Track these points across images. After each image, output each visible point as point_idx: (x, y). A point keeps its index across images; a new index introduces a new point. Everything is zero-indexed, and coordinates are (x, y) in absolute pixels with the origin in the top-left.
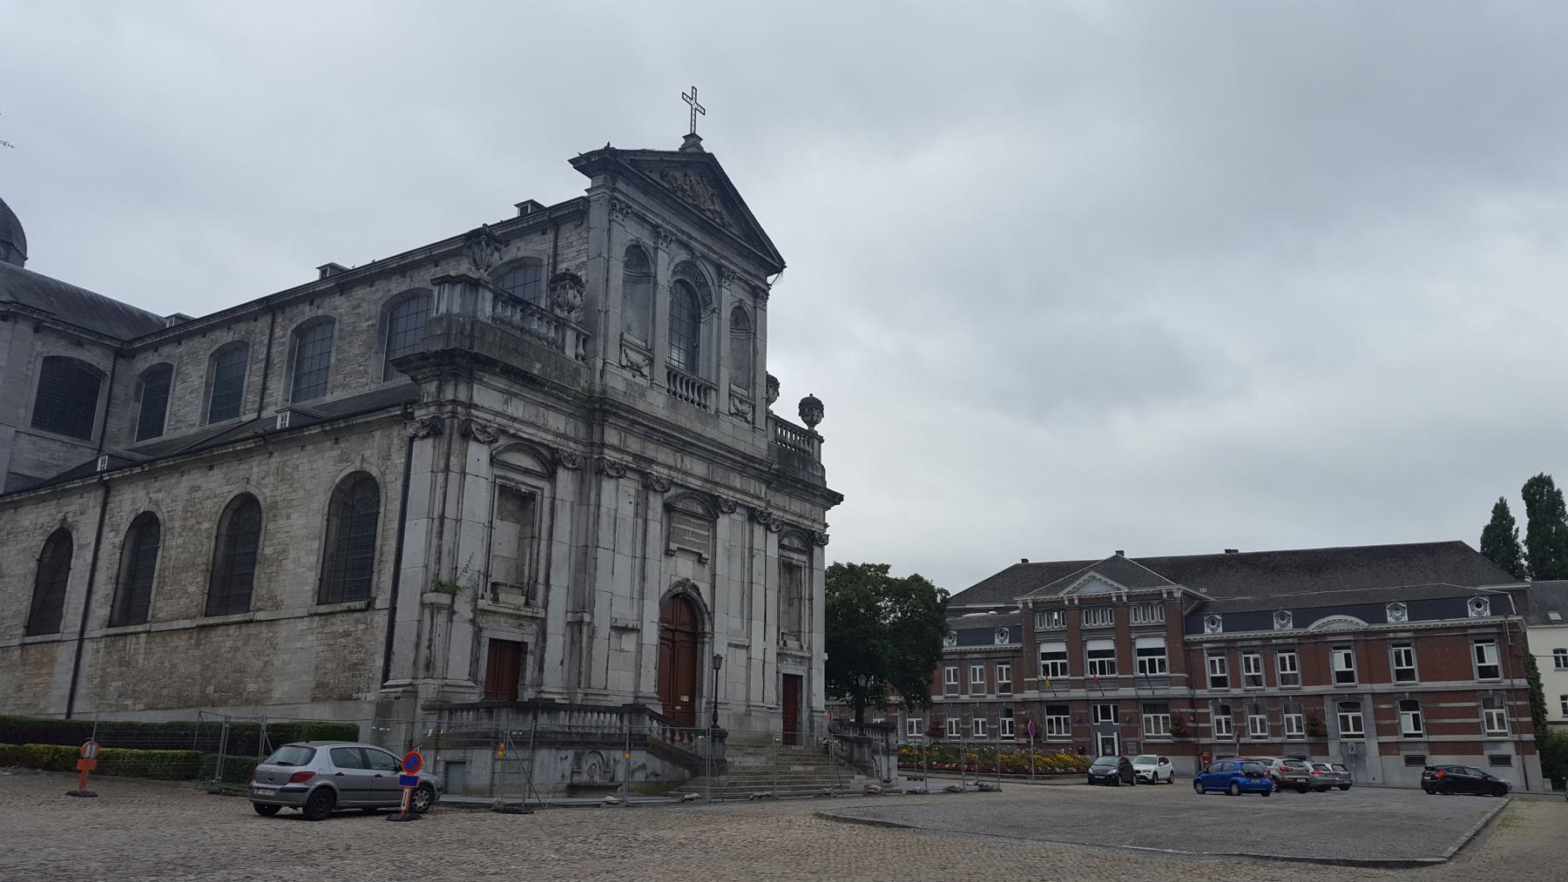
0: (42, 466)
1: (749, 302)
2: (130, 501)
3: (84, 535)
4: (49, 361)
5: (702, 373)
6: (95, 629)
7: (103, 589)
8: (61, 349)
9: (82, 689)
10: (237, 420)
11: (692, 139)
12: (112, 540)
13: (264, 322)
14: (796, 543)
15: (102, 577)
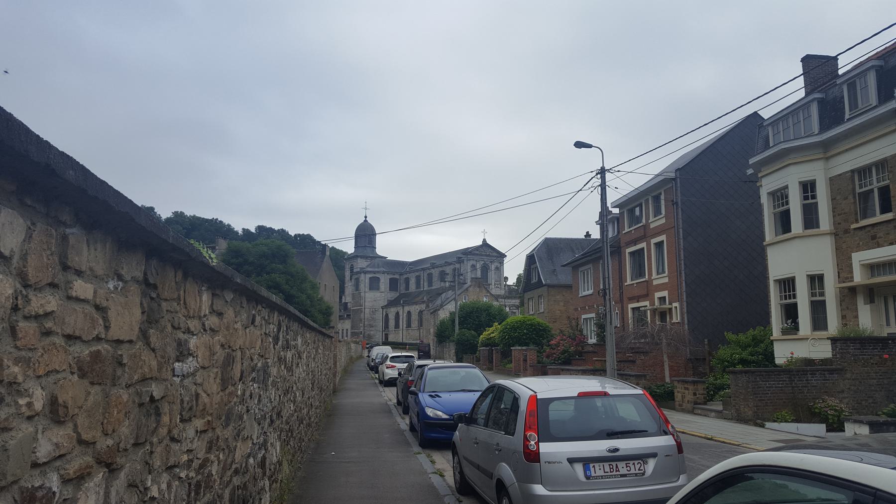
0: (391, 298)
1: (499, 265)
2: (407, 309)
3: (401, 313)
4: (391, 279)
5: (489, 283)
6: (404, 329)
7: (405, 322)
8: (392, 276)
9: (404, 337)
10: (420, 290)
11: (484, 240)
12: (405, 315)
13: (422, 272)
14: (514, 308)
15: (404, 320)
